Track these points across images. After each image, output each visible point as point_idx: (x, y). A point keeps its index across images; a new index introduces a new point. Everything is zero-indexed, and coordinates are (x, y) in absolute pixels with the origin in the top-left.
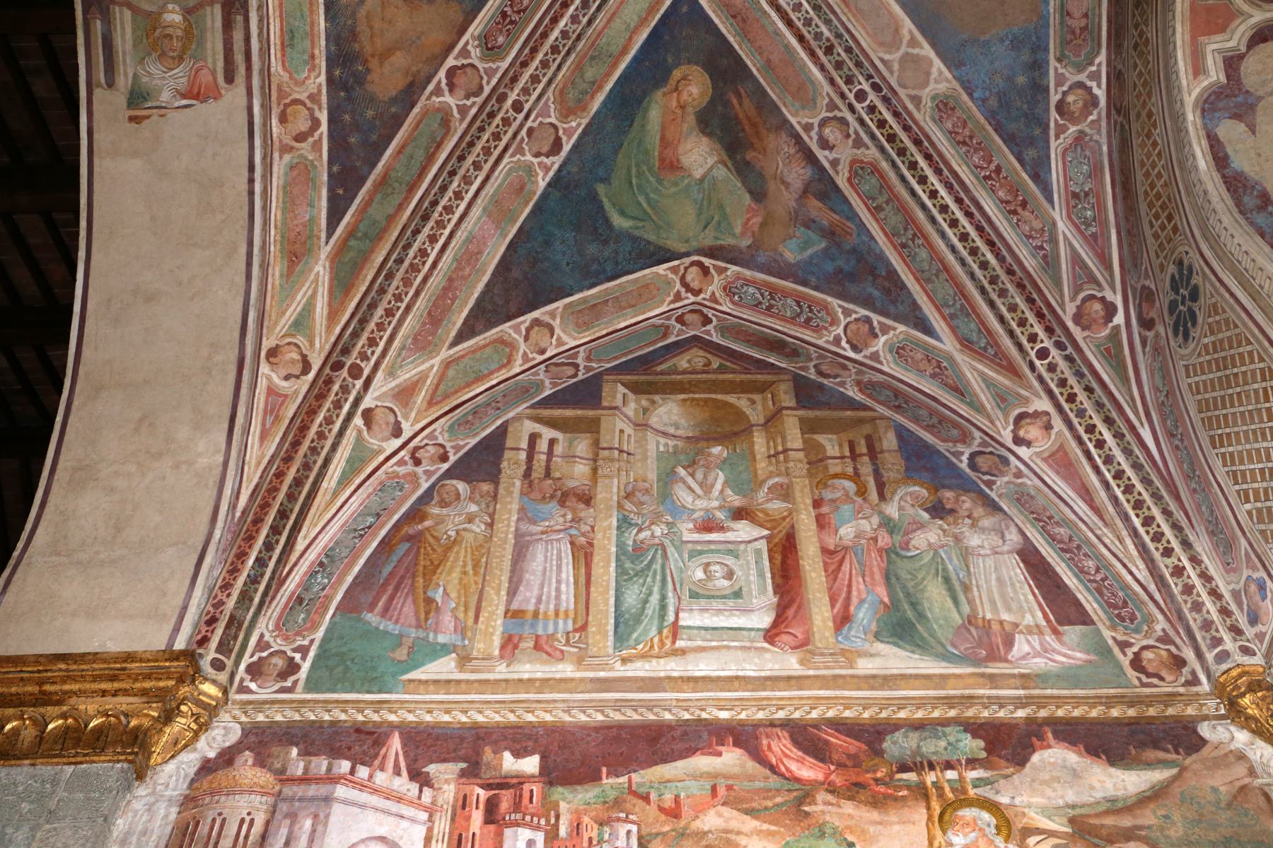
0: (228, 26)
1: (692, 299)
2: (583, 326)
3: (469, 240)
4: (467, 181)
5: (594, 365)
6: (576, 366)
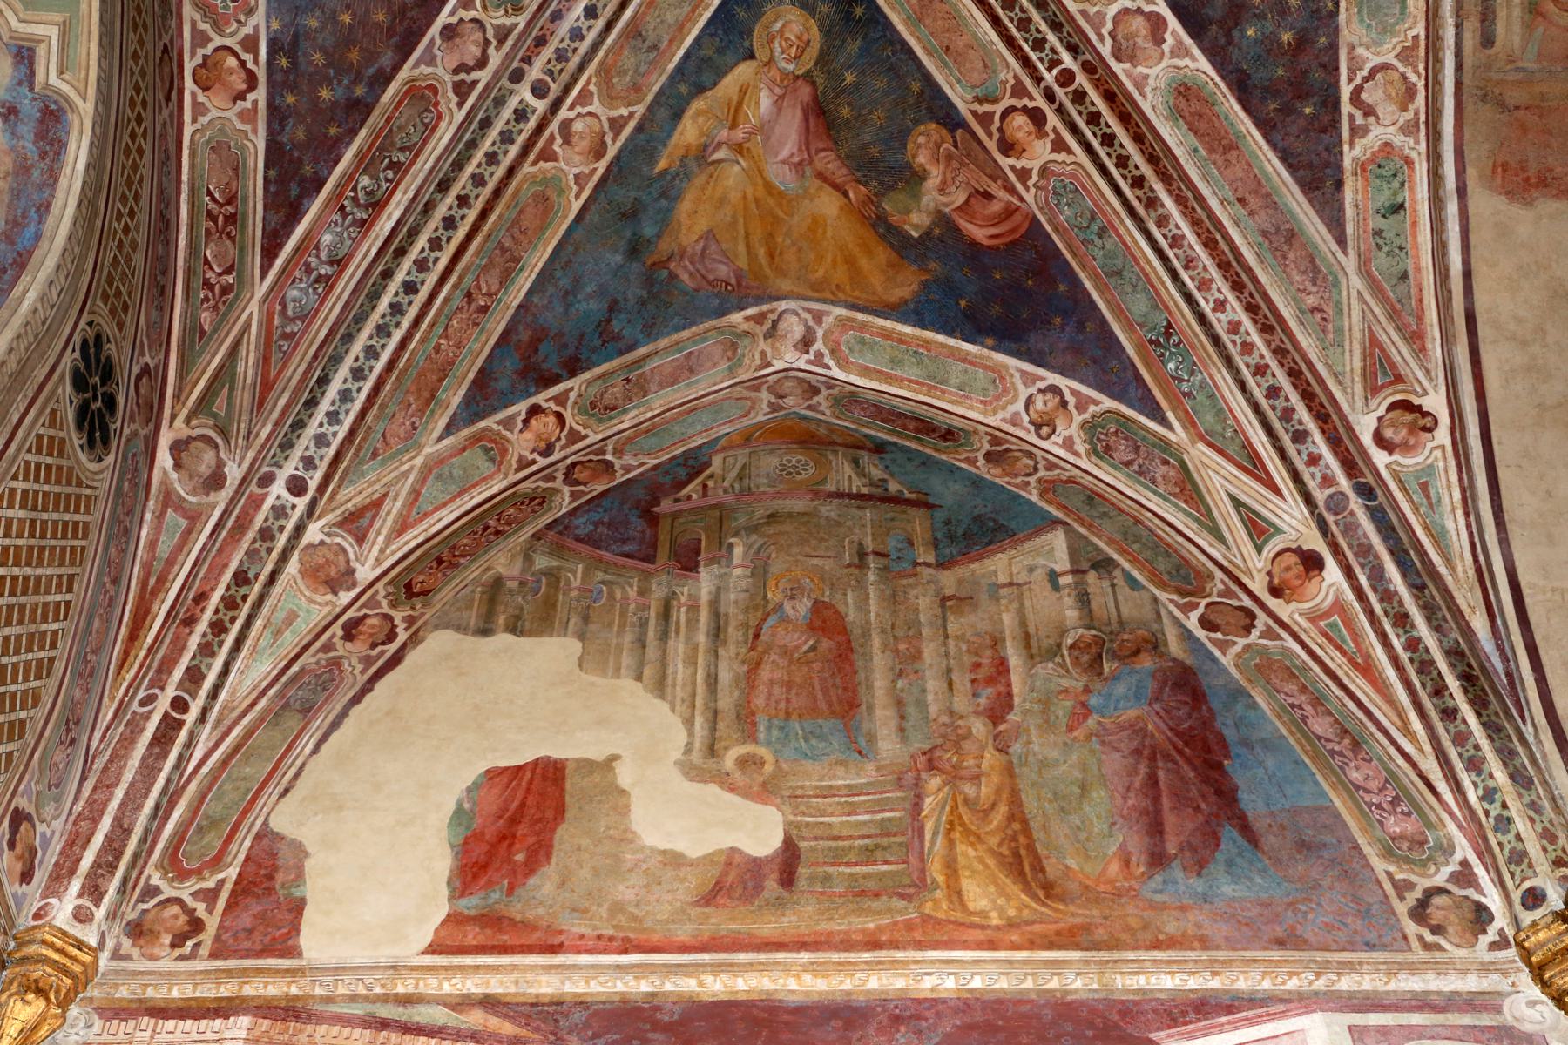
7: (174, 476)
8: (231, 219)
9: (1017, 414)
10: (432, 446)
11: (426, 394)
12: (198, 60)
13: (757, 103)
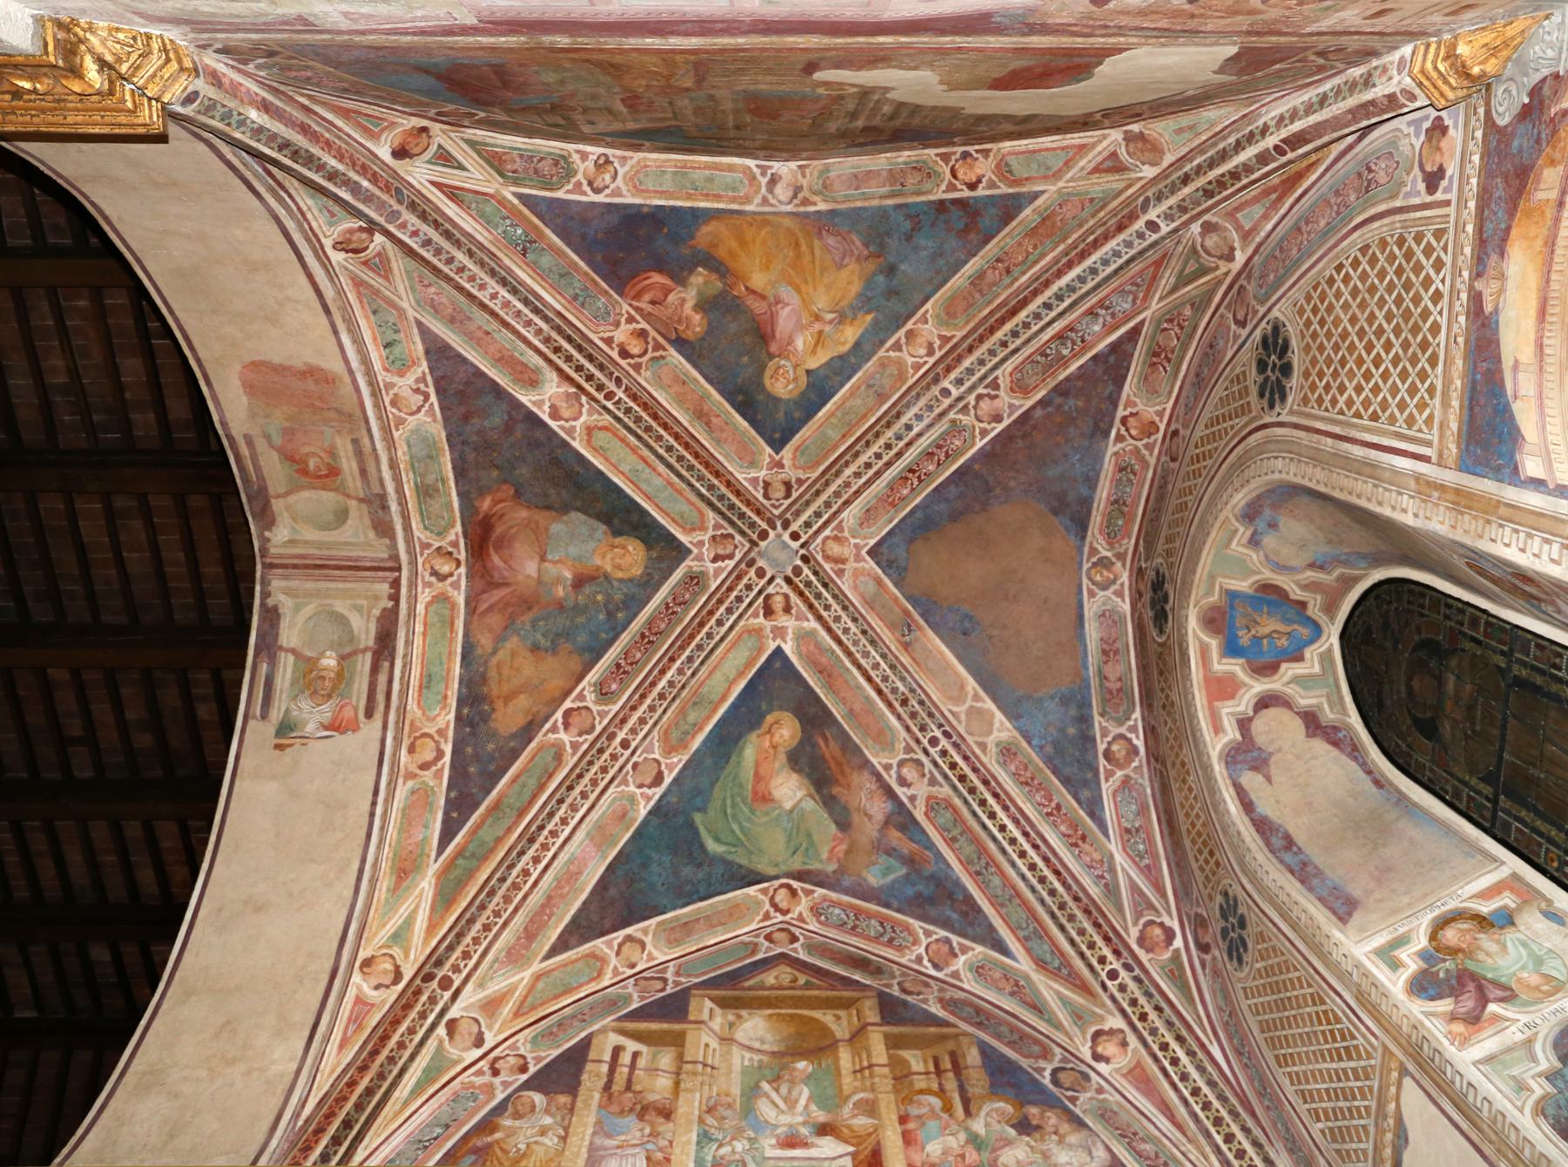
0: (375, 670)
1: (780, 918)
4: (574, 808)
6: (665, 980)
7: (1236, 245)
8: (1156, 354)
10: (1051, 189)
11: (1048, 223)
12: (1153, 438)
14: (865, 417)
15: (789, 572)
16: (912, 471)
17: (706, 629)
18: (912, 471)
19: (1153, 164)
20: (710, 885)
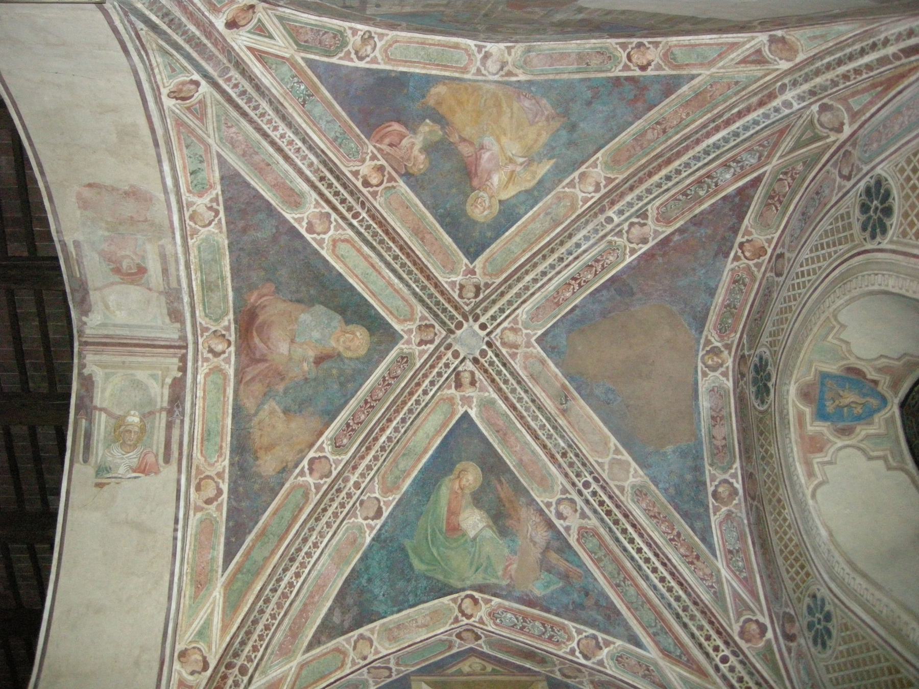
1: (466, 621)
2: (393, 639)
3: (319, 576)
4: (322, 535)
5: (403, 669)
6: (390, 669)
8: (772, 197)
9: (380, 41)
10: (704, 74)
12: (762, 258)
13: (500, 180)
14: (541, 237)
15: (477, 355)
16: (574, 279)
17: (415, 397)
18: (574, 279)
19: (788, 60)
20: (416, 595)
